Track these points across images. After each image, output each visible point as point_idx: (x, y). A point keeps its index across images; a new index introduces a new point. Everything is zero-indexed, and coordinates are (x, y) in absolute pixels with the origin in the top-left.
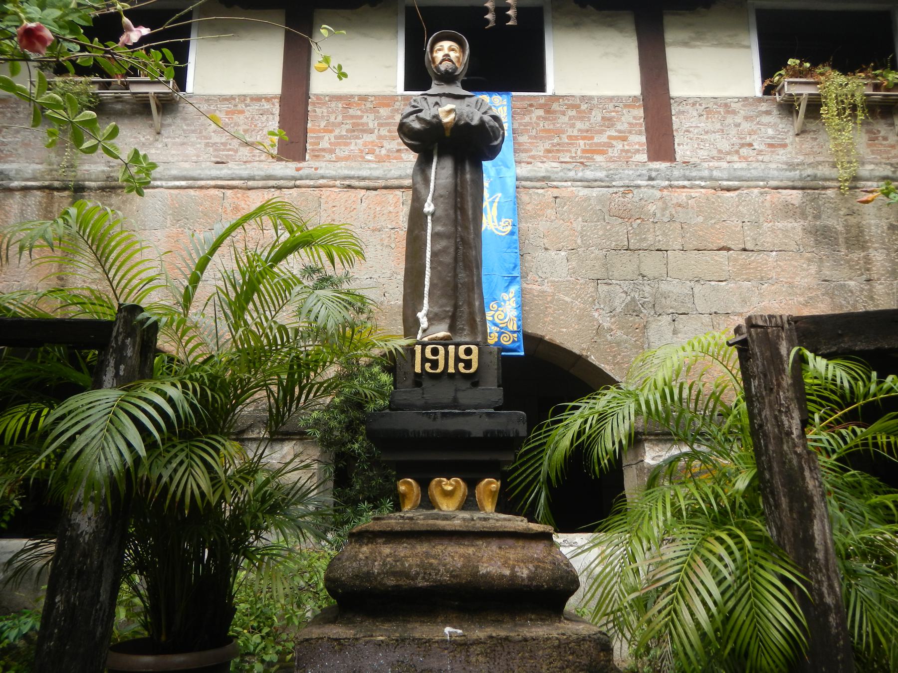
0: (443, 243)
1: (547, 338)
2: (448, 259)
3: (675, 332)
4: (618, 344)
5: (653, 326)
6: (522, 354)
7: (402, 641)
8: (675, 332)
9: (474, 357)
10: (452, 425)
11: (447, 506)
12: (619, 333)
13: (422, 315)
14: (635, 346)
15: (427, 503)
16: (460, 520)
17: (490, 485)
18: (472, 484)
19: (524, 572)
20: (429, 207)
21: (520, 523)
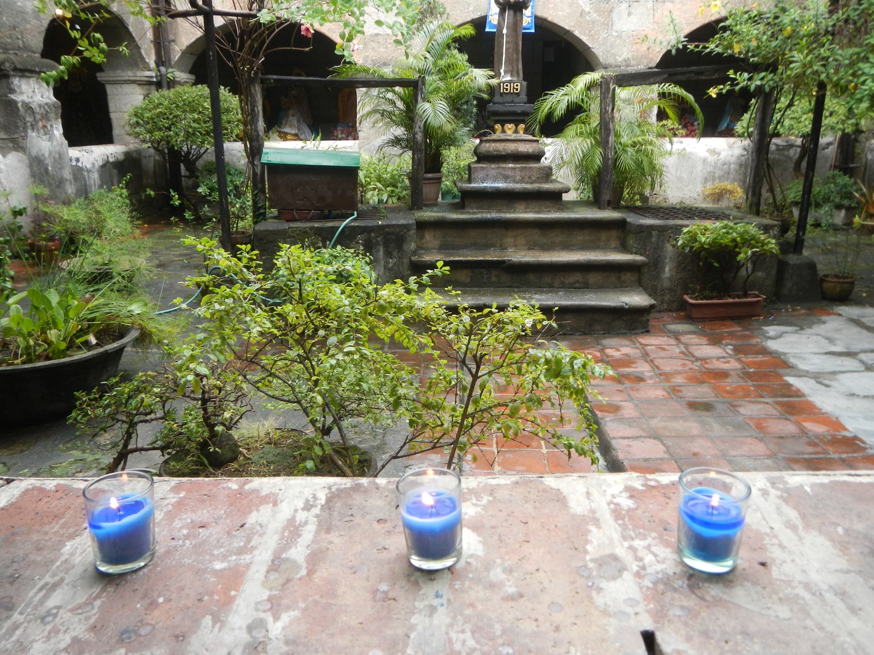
0: (509, 45)
1: (549, 19)
2: (511, 51)
3: (629, 14)
4: (593, 22)
5: (616, 10)
6: (533, 31)
7: (498, 168)
8: (629, 14)
9: (519, 87)
10: (512, 109)
11: (509, 132)
12: (594, 15)
13: (502, 71)
14: (603, 24)
15: (503, 131)
16: (514, 136)
17: (522, 126)
18: (517, 126)
19: (531, 150)
20: (505, 31)
21: (530, 137)
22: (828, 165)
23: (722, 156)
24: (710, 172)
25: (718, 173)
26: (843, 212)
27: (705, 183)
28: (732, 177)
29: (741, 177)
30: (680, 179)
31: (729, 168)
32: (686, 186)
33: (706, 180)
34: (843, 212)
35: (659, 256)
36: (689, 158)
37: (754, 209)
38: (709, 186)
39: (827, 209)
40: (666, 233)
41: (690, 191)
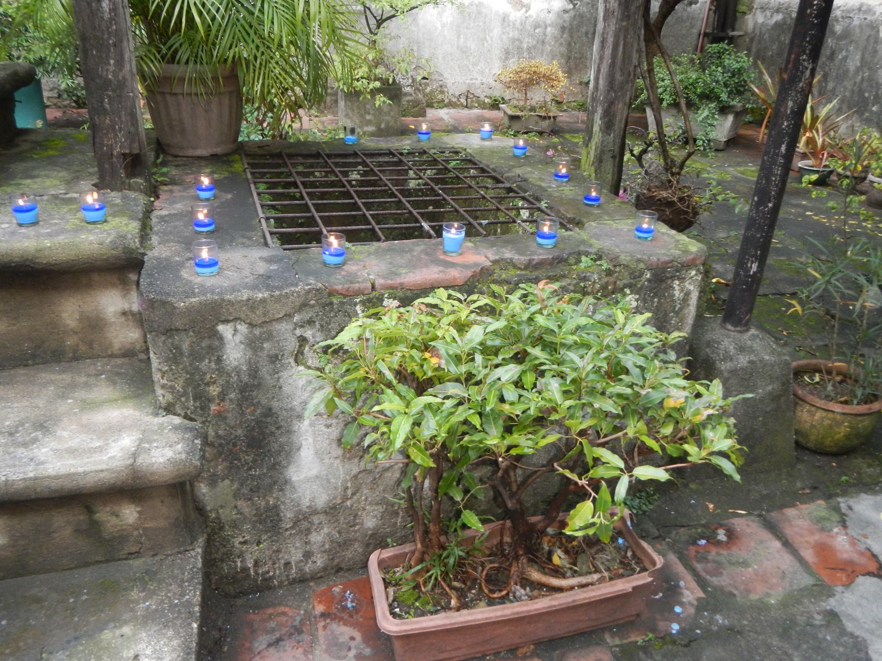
22: (695, 31)
23: (533, 12)
24: (514, 40)
25: (527, 42)
26: (730, 118)
27: (507, 59)
28: (548, 48)
29: (563, 49)
30: (464, 51)
31: (545, 34)
32: (475, 65)
33: (507, 53)
34: (730, 118)
35: (269, 412)
36: (479, 13)
37: (609, 166)
38: (513, 64)
39: (706, 113)
40: (284, 328)
41: (482, 72)
